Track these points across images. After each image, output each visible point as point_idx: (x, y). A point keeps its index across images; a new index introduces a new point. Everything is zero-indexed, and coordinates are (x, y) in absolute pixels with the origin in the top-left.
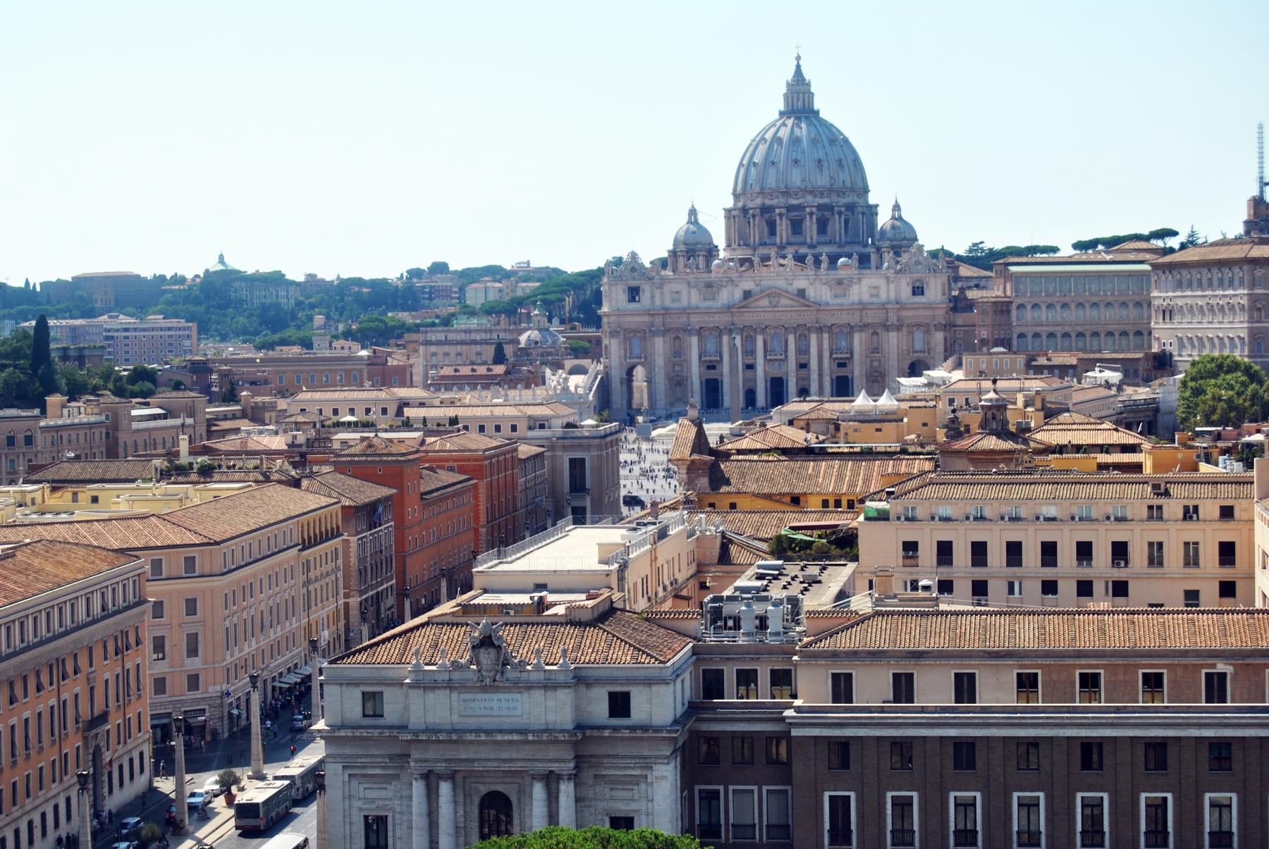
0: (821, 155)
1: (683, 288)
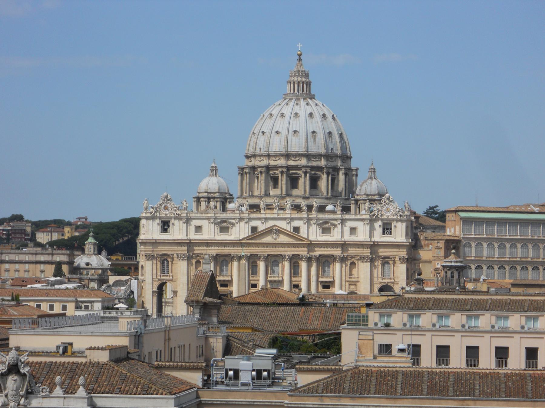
1: (205, 224)
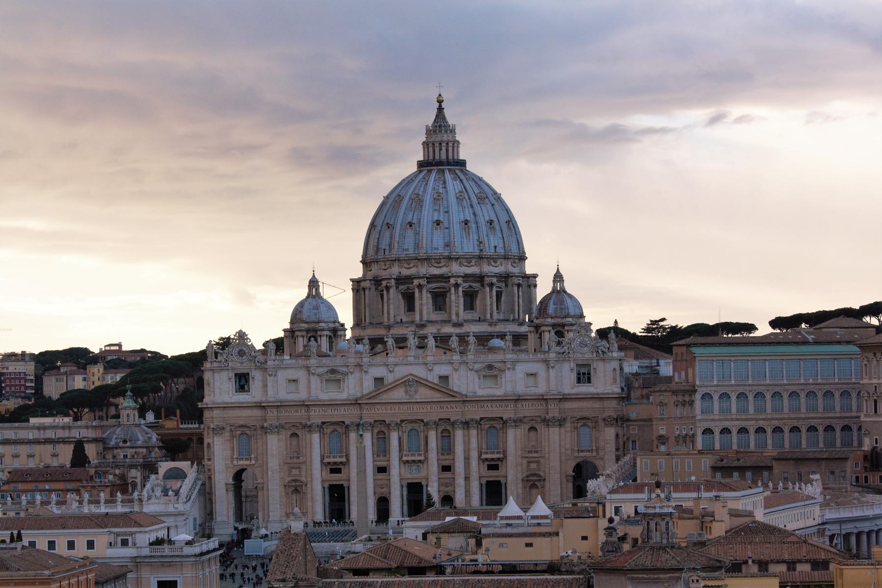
0: (469, 217)
1: (301, 375)
